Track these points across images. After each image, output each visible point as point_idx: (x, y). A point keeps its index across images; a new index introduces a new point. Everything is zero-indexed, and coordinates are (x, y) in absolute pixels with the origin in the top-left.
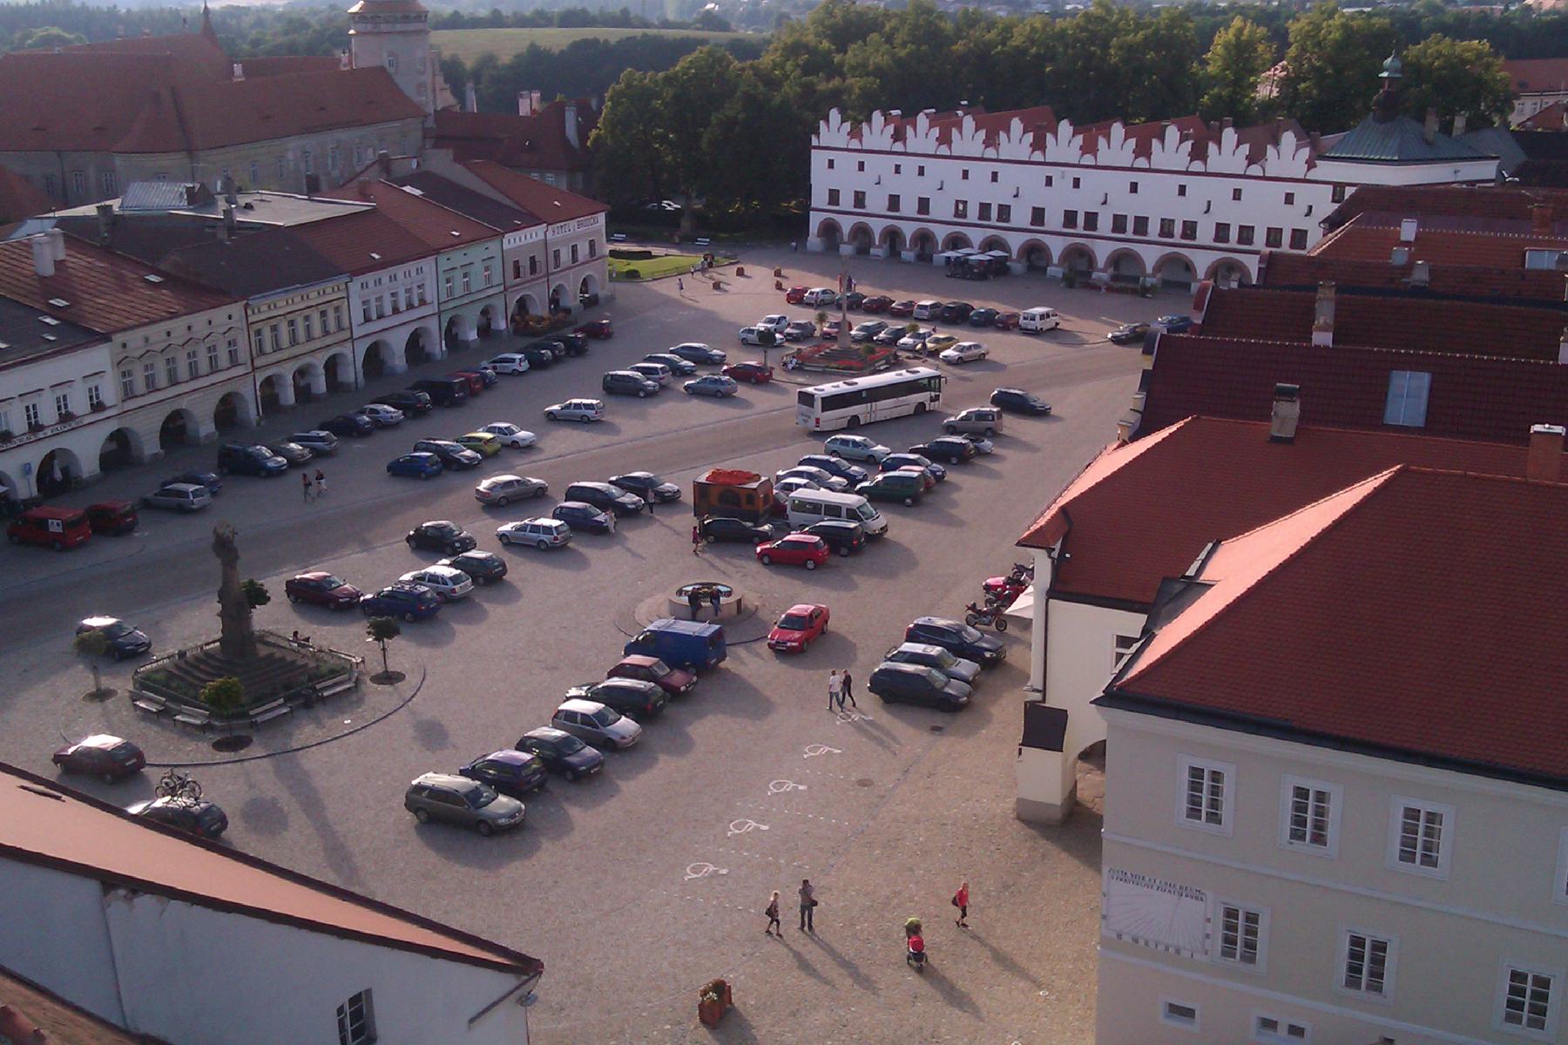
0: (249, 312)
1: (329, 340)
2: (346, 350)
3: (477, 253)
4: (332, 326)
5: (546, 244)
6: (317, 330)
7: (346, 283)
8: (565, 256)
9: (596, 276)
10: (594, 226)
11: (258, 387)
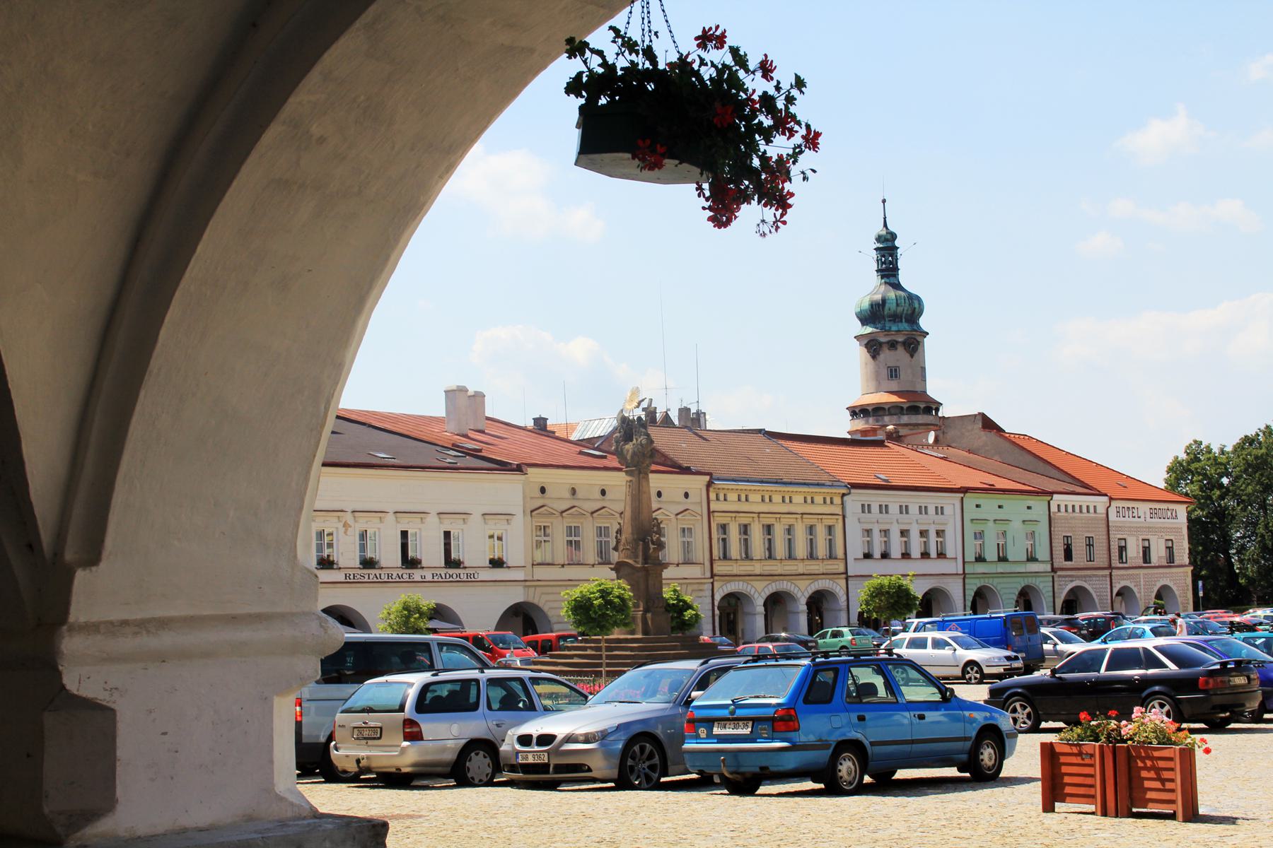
0: (713, 496)
1: (814, 567)
2: (838, 587)
3: (1015, 508)
4: (821, 550)
5: (1108, 526)
6: (801, 549)
7: (844, 495)
8: (1134, 552)
9: (1171, 585)
10: (1170, 520)
11: (716, 603)
